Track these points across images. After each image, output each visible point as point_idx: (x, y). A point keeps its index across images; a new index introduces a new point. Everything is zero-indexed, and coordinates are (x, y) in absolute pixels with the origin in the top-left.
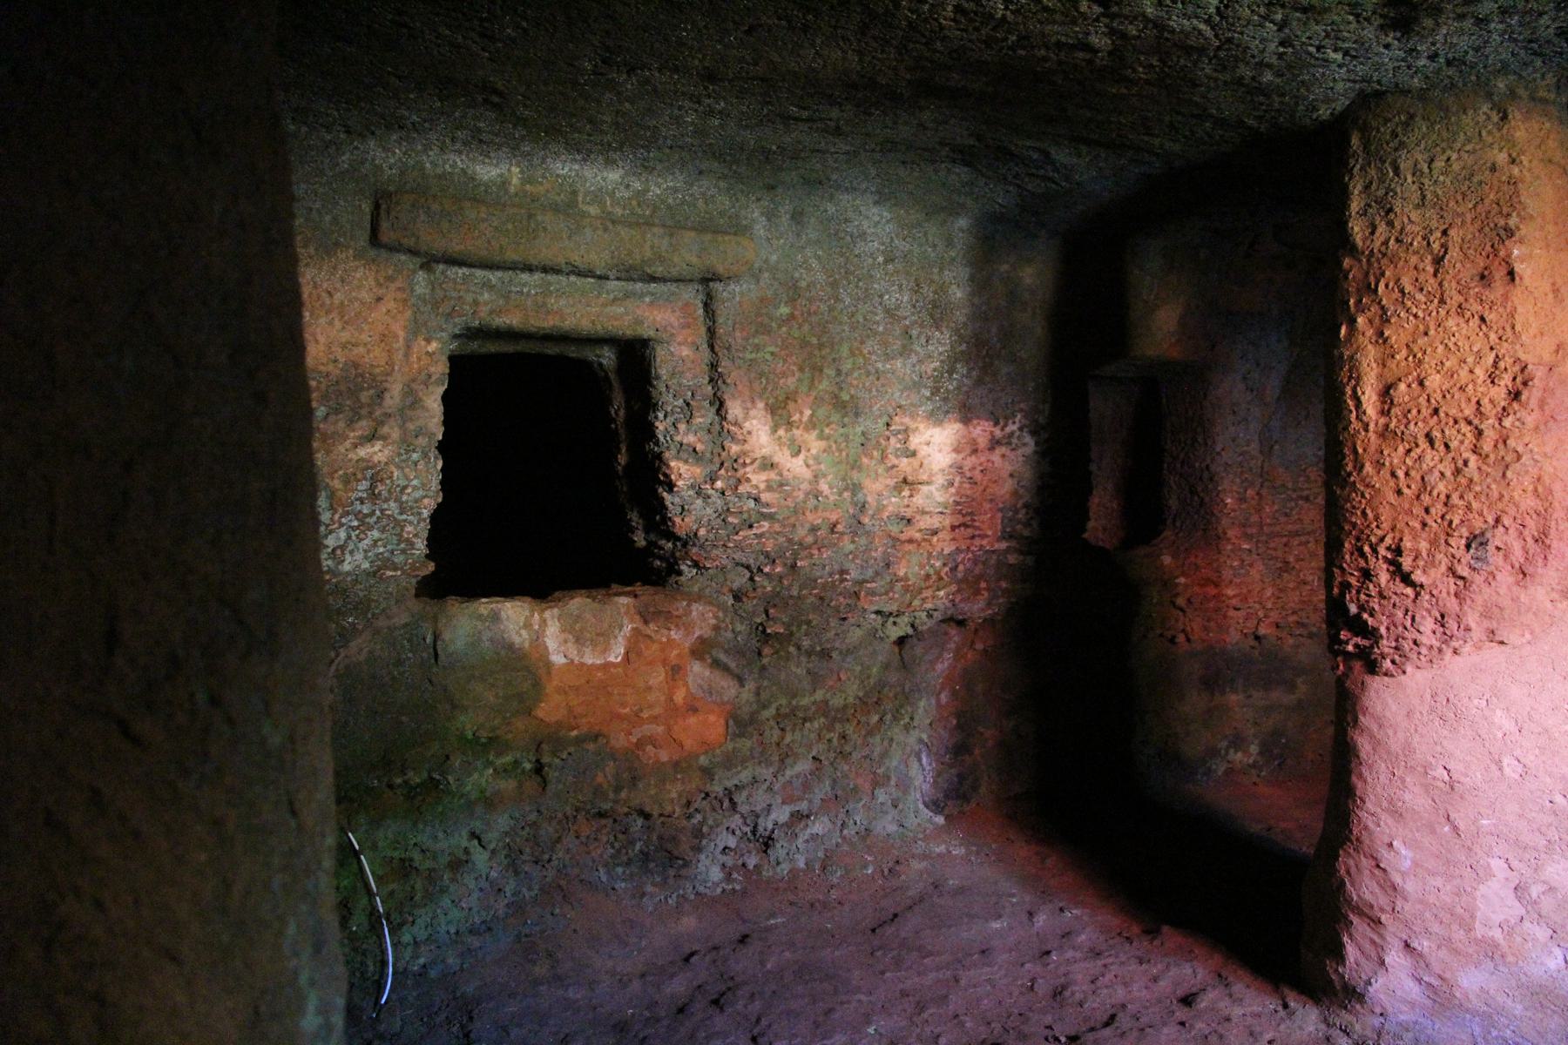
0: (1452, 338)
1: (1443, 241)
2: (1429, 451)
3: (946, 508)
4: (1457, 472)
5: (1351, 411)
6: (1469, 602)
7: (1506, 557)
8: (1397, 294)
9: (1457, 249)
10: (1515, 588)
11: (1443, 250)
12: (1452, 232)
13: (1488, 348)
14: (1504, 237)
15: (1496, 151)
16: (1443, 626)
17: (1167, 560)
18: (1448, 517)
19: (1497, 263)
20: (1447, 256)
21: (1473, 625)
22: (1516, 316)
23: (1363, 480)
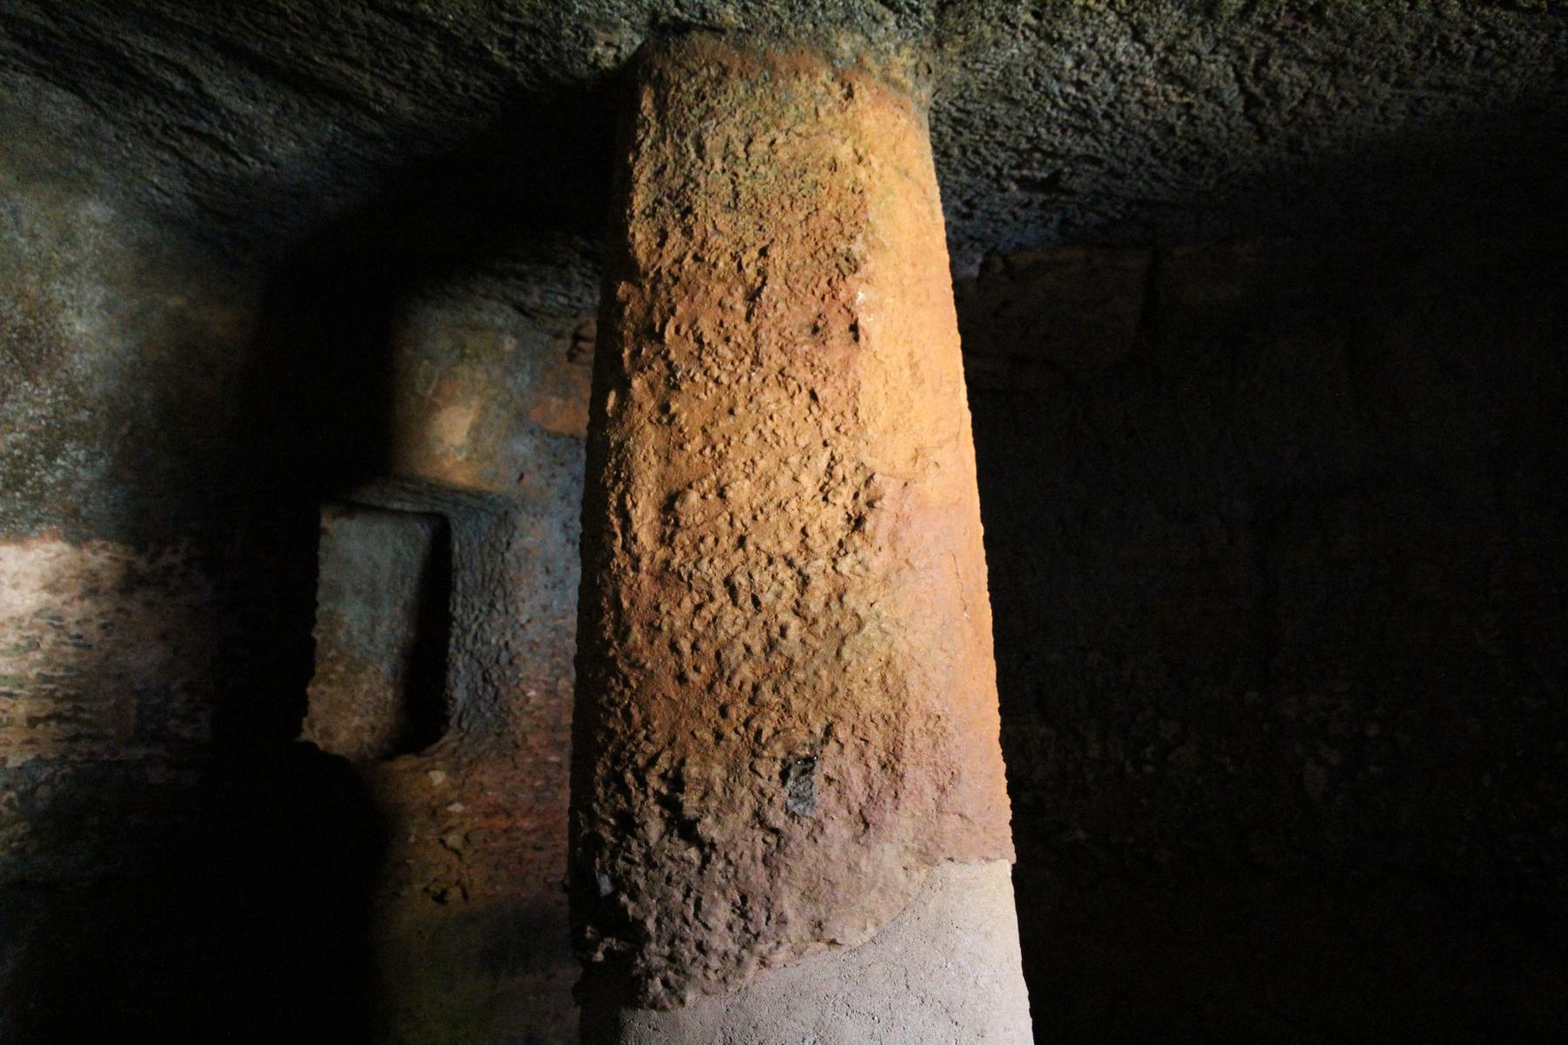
0: (769, 422)
1: (760, 264)
2: (729, 607)
3: (21, 687)
4: (771, 646)
5: (615, 536)
6: (784, 873)
7: (840, 794)
8: (692, 345)
9: (780, 280)
10: (853, 848)
11: (760, 279)
12: (774, 252)
13: (820, 442)
14: (846, 271)
15: (837, 142)
16: (743, 915)
17: (438, 777)
18: (755, 724)
19: (835, 310)
20: (765, 290)
21: (790, 914)
22: (860, 396)
23: (627, 656)
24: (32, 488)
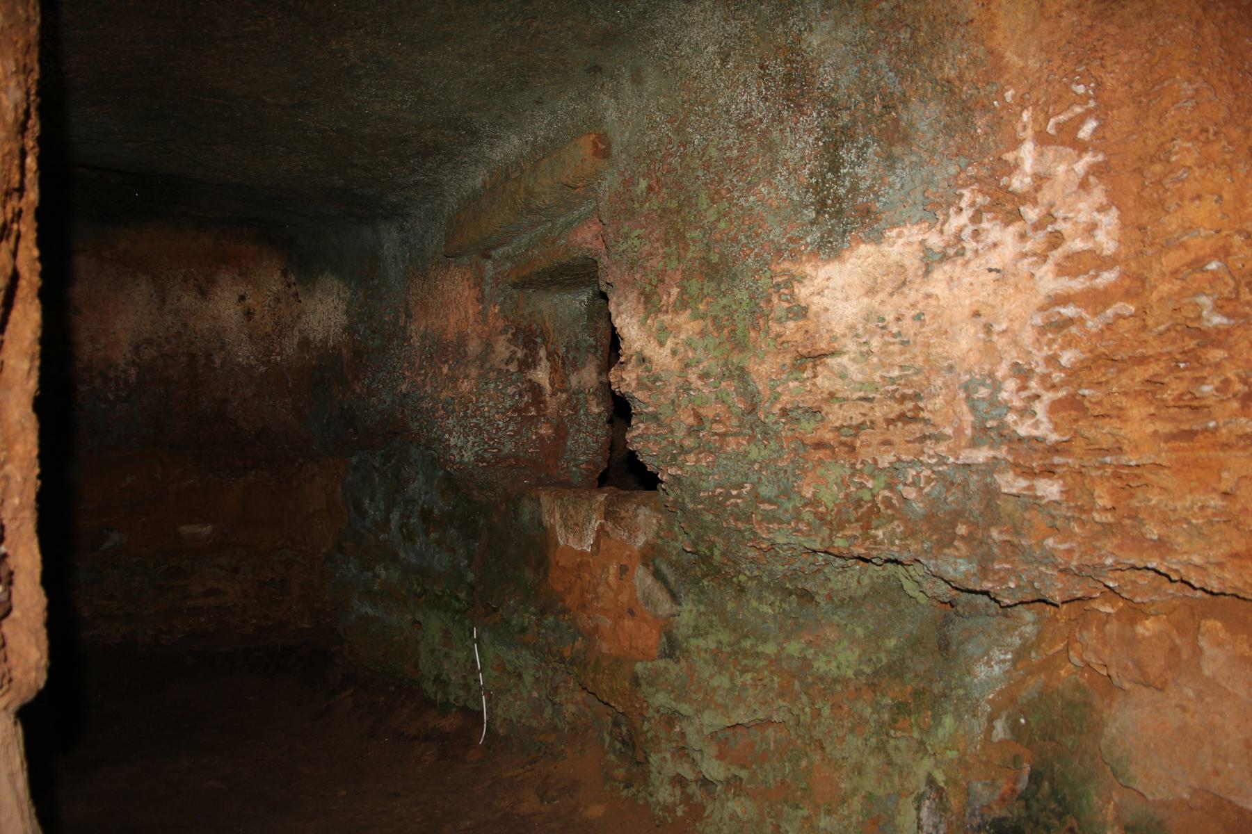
24: (833, 205)
